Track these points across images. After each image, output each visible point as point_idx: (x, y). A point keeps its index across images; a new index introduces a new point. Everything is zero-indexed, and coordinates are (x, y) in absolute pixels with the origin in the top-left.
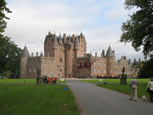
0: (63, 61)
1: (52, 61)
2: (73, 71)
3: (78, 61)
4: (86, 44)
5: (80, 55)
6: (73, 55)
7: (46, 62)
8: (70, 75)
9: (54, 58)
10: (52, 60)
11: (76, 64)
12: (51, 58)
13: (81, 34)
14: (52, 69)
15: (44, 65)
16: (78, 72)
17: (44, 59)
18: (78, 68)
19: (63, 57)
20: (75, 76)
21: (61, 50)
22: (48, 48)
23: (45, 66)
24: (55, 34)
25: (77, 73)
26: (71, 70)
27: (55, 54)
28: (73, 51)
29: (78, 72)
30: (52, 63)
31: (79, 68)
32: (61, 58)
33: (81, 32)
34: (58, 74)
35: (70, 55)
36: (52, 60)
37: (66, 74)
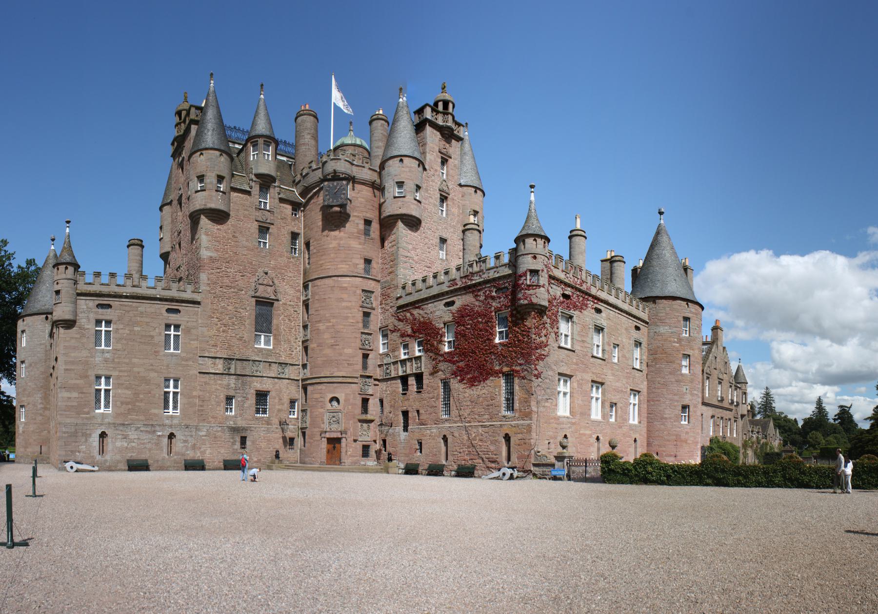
0: (279, 319)
1: (173, 318)
6: (367, 271)
7: (108, 323)
8: (338, 440)
9: (188, 295)
10: (174, 306)
14: (171, 389)
15: (85, 353)
16: (405, 414)
17: (92, 303)
18: (404, 379)
20: (382, 456)
21: (264, 230)
23: (98, 359)
26: (349, 395)
28: (367, 233)
29: (405, 414)
30: (172, 332)
31: (412, 381)
32: (267, 293)
34: (234, 430)
35: (343, 269)
36: (174, 306)
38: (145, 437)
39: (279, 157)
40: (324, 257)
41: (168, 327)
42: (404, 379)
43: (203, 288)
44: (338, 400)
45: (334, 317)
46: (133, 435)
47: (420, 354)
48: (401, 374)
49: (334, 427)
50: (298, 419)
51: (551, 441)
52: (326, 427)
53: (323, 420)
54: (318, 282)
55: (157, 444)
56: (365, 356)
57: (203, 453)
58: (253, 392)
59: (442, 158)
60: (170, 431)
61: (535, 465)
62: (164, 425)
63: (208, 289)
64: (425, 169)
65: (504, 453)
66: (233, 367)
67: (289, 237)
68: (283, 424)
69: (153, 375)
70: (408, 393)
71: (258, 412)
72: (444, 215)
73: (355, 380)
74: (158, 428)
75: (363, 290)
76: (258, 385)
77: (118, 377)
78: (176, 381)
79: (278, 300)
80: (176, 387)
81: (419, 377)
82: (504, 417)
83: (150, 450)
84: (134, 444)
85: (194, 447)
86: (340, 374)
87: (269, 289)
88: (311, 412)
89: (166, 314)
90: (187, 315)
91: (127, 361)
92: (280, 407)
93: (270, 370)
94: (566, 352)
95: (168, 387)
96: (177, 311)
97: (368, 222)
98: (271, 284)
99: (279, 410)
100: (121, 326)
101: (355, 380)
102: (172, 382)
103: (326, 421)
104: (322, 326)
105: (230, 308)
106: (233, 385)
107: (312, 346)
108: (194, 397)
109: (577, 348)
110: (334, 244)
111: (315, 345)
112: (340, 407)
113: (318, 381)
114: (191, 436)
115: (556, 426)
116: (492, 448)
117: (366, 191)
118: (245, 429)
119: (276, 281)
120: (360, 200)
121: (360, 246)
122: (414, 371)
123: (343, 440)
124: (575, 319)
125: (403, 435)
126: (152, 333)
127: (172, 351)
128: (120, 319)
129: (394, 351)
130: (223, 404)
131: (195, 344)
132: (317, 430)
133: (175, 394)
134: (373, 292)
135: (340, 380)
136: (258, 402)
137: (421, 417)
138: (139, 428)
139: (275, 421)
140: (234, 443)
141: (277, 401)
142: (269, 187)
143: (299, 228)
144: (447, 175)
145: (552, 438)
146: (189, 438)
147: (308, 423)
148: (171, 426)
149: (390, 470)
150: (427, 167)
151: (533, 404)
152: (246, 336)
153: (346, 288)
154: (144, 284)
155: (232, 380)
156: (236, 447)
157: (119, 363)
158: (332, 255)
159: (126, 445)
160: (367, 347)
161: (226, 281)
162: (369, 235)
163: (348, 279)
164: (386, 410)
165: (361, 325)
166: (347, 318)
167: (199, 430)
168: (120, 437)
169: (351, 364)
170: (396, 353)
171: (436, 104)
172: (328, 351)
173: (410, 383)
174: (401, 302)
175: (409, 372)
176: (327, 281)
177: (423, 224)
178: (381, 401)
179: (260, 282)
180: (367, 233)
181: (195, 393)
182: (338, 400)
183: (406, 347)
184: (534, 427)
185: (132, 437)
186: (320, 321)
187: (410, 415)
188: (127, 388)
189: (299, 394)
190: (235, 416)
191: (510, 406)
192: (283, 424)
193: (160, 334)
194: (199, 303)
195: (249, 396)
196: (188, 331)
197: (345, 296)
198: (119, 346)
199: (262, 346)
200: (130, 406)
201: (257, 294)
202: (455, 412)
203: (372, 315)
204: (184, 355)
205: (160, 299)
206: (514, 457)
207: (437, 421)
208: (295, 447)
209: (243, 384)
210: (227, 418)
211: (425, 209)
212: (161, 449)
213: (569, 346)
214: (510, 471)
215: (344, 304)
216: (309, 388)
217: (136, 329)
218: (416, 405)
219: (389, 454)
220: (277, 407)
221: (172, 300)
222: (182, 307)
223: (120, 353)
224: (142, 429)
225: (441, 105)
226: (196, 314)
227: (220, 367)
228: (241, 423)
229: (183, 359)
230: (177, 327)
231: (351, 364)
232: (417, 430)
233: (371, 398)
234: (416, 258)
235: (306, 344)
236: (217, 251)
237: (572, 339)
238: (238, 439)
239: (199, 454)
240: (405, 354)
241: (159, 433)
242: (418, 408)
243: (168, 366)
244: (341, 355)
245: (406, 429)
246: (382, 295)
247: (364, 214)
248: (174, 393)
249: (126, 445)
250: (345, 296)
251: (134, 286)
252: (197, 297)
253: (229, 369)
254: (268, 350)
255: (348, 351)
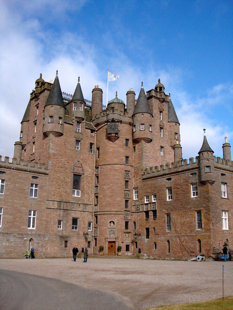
0: (84, 183)
1: (35, 181)
2: (127, 227)
3: (149, 182)
4: (177, 123)
5: (154, 157)
6: (126, 163)
9: (43, 170)
10: (36, 175)
11: (142, 199)
12: (29, 168)
13: (160, 89)
14: (32, 216)
16: (148, 229)
18: (147, 213)
19: (89, 171)
21: (78, 141)
22: (31, 137)
24: (57, 80)
25: (144, 237)
26: (120, 221)
27: (51, 151)
28: (127, 145)
29: (148, 229)
31: (151, 214)
32: (78, 171)
33: (159, 81)
34: (62, 237)
35: (116, 161)
36: (36, 175)
37: (98, 238)
38: (17, 240)
39: (86, 107)
40: (106, 156)
41: (32, 185)
42: (147, 213)
43: (49, 167)
44: (114, 223)
45: (111, 183)
46: (12, 239)
47: (155, 201)
48: (145, 210)
49: (112, 236)
50: (92, 232)
51: (220, 242)
52: (107, 236)
53: (106, 232)
54: (104, 167)
55: (24, 244)
56: (127, 201)
57: (46, 249)
58: (71, 218)
59: (160, 111)
60: (31, 237)
61: (213, 254)
62: (28, 234)
63: (52, 168)
64: (153, 117)
65: (198, 249)
66: (62, 206)
67: (89, 145)
68: (86, 234)
69: (24, 208)
70: (149, 219)
71: (73, 228)
72: (162, 136)
73: (122, 213)
74: (25, 236)
75: (125, 171)
76: (74, 215)
77: (7, 209)
78: (34, 212)
79: (84, 174)
80: (34, 215)
81: (155, 212)
82: (197, 231)
83: (20, 247)
84: (12, 244)
85: (42, 246)
86: (115, 210)
87: (80, 169)
88: (99, 228)
89: (31, 179)
90: (41, 180)
91: (11, 201)
92: (84, 226)
93: (79, 207)
94: (225, 200)
95: (30, 215)
96: (36, 178)
97: (127, 140)
98: (81, 166)
99: (83, 228)
100: (9, 183)
101: (122, 213)
102: (32, 212)
103: (108, 233)
104: (105, 187)
105: (62, 177)
106: (62, 215)
107: (100, 196)
108: (43, 220)
109: (230, 197)
110: (111, 150)
111: (102, 196)
112: (115, 226)
113: (103, 213)
114: (41, 240)
115: (222, 235)
116: (192, 246)
117: (127, 127)
118: (67, 237)
119: (83, 165)
120: (124, 130)
121: (124, 151)
122: (152, 209)
123: (117, 242)
124: (228, 184)
125: (146, 240)
126: (24, 188)
127: (33, 197)
128: (9, 179)
129: (141, 199)
130: (57, 224)
131: (45, 194)
132: (103, 237)
133: (34, 218)
134: (130, 171)
135: (114, 213)
136: (73, 224)
137: (156, 231)
138: (15, 236)
139: (81, 233)
140: (61, 244)
141: (82, 223)
142: (81, 122)
143: (94, 141)
144: (162, 118)
145: (220, 241)
146: (40, 241)
147: (98, 234)
148: (31, 235)
149: (140, 257)
150: (154, 116)
151: (211, 225)
152: (68, 191)
153: (117, 170)
154: (22, 164)
155: (62, 212)
156: (62, 246)
157: (7, 201)
158: (111, 155)
159: (8, 244)
160: (127, 197)
161: (60, 164)
162: (128, 146)
163: (118, 166)
164: (137, 227)
165: (124, 187)
166: (118, 184)
167: (45, 237)
168: (5, 240)
169: (120, 206)
170: (143, 200)
171: (156, 88)
172: (108, 199)
173: (149, 215)
174: (144, 177)
175: (149, 209)
176: (108, 166)
177: (153, 141)
178: (135, 223)
179: (76, 165)
180: (127, 145)
181: (44, 219)
182: (114, 223)
183: (148, 197)
184: (212, 236)
185: (11, 240)
186: (104, 185)
187: (150, 230)
188: (10, 215)
189: (93, 220)
190: (62, 230)
191: (200, 226)
192: (86, 234)
193: (28, 188)
194: (48, 174)
195: (69, 220)
196: (41, 188)
197: (117, 173)
198: (8, 193)
199: (76, 196)
200: (11, 224)
201: (75, 171)
202: (173, 229)
203: (129, 182)
204: (39, 199)
205: (29, 172)
206: (203, 250)
207: (164, 234)
208: (91, 246)
209: (67, 214)
210: (58, 231)
211: (153, 134)
212: (26, 247)
213: (226, 197)
214: (201, 257)
215: (116, 177)
216: (99, 216)
217: (17, 185)
218: (153, 225)
219: (140, 249)
220: (82, 226)
221: (35, 172)
222: (40, 176)
223: (8, 196)
224: (17, 236)
225: (158, 88)
226: (46, 180)
227: (56, 206)
228: (65, 234)
229: (39, 201)
230: (36, 185)
231: (120, 206)
232: (153, 237)
233: (129, 221)
234: (150, 156)
235: (97, 195)
236: (57, 150)
237: (227, 193)
238: (64, 242)
239: (44, 250)
240: (147, 201)
241: (25, 239)
242: (154, 227)
243: (31, 204)
244: (115, 201)
245: (148, 237)
246: (135, 173)
247: (126, 136)
248: (33, 218)
249: (8, 244)
250: (117, 173)
251: (17, 164)
252: (47, 172)
253: (60, 207)
254: (79, 198)
255: (119, 199)
